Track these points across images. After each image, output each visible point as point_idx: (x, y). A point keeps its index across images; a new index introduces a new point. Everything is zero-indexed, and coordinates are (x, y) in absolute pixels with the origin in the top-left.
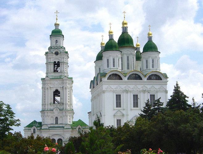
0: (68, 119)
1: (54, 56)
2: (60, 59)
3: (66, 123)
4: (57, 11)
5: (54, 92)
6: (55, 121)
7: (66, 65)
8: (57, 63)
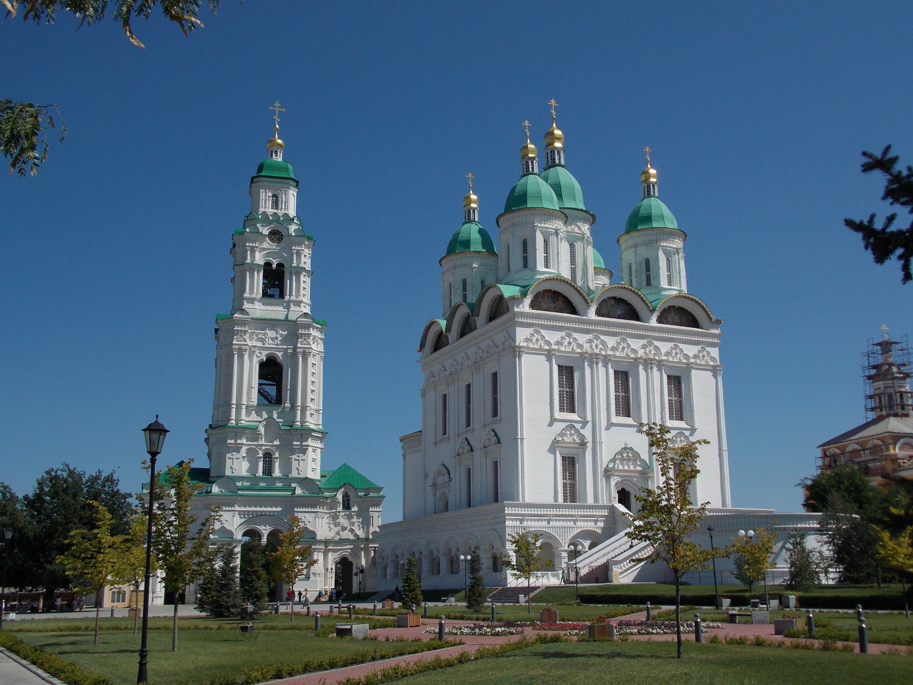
0: (310, 460)
1: (267, 244)
3: (302, 476)
5: (262, 365)
6: (261, 464)
8: (274, 266)
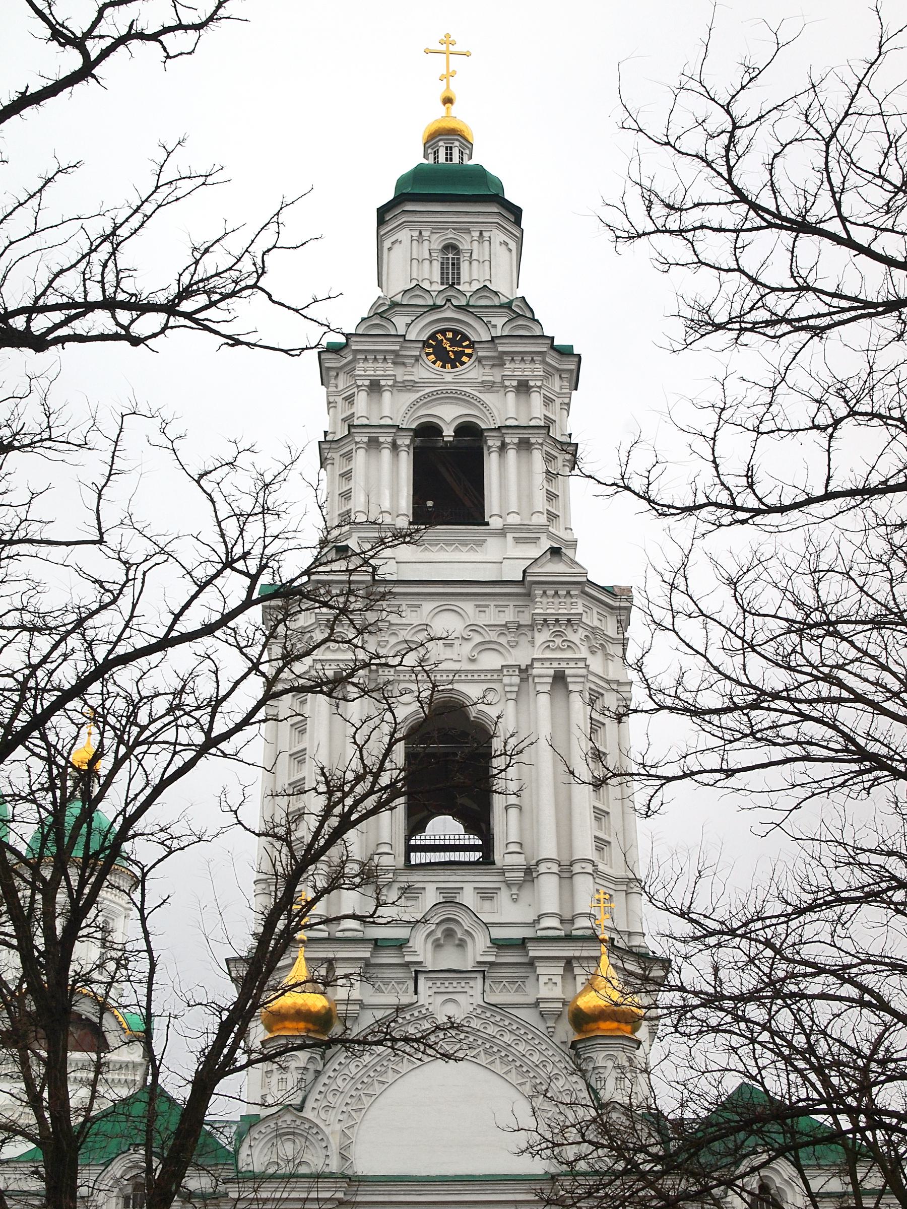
2: (488, 398)
4: (447, 40)
7: (549, 458)
